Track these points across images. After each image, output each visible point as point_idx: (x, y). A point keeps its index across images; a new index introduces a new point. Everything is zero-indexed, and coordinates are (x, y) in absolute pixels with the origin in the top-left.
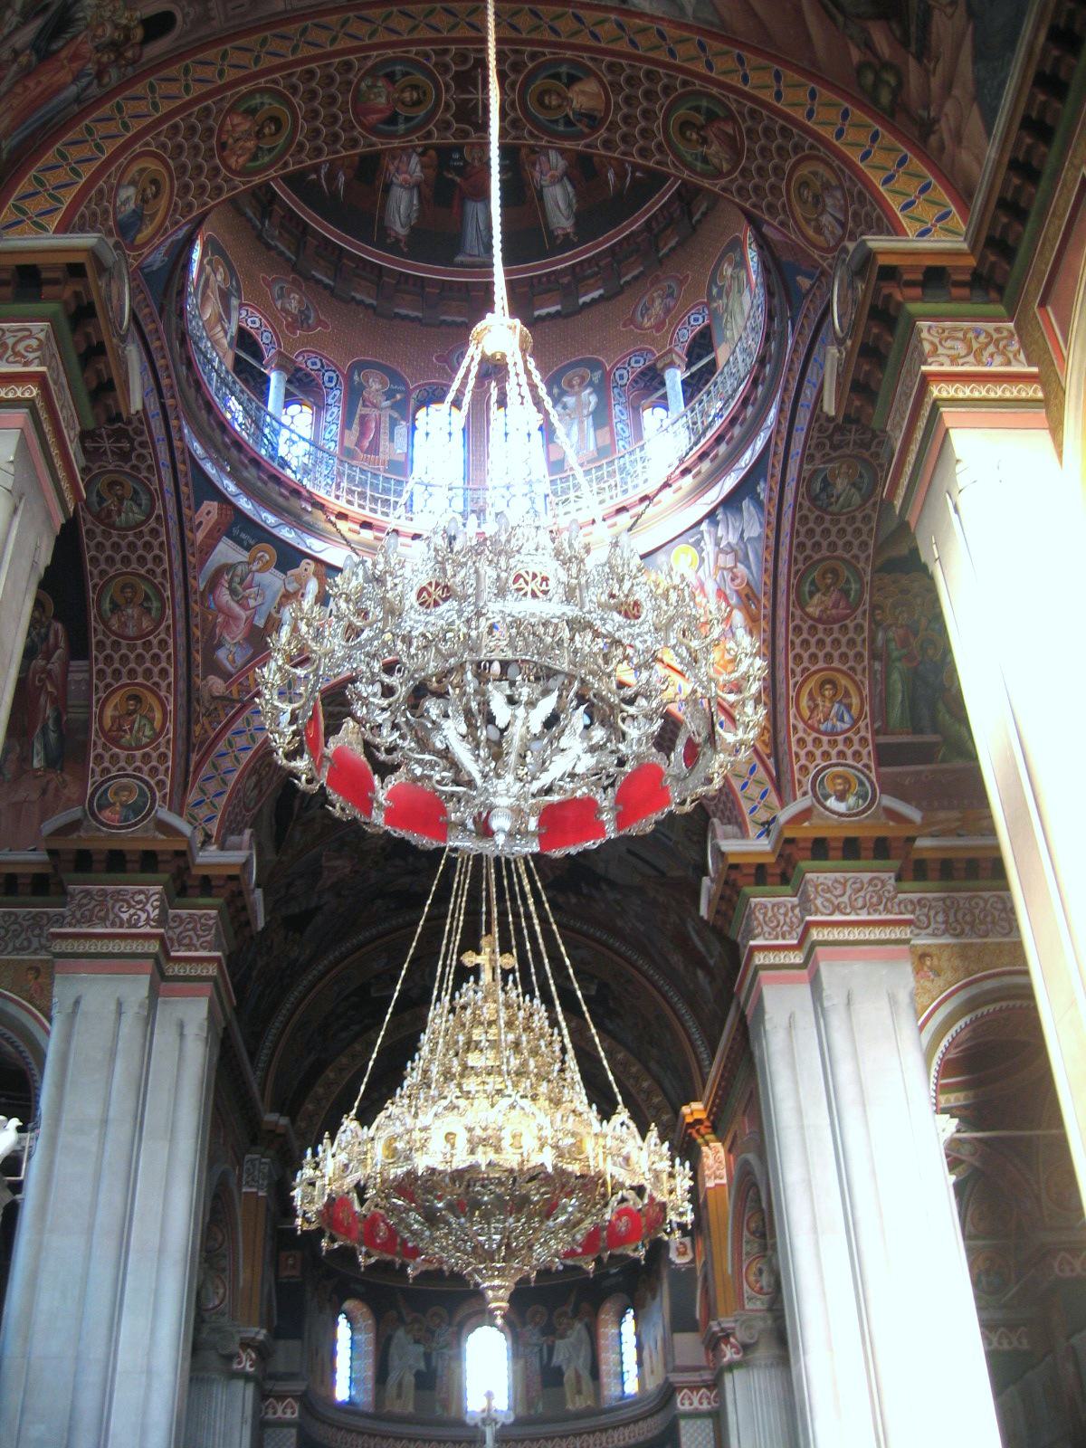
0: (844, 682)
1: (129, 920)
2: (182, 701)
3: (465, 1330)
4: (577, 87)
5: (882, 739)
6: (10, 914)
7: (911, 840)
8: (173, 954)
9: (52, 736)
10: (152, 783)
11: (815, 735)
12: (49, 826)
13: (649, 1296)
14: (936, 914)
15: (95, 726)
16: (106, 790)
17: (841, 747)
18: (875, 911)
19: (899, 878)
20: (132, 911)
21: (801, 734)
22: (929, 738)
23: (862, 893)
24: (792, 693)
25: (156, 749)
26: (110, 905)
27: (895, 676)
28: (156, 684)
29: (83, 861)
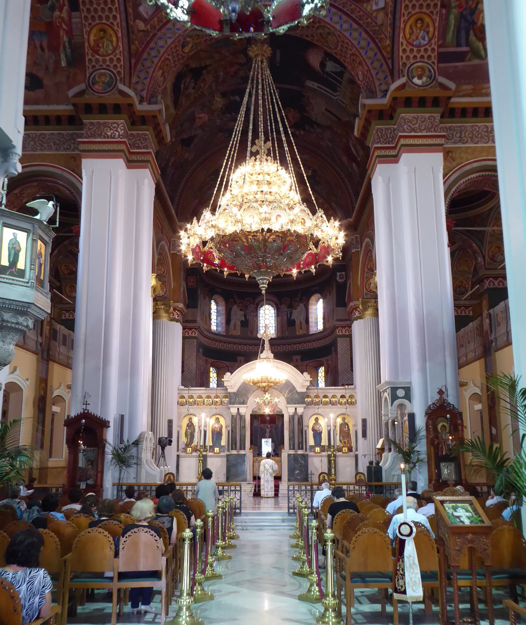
0: (427, 19)
1: (111, 136)
2: (125, 32)
5: (442, 50)
6: (60, 133)
7: (449, 98)
8: (131, 151)
9: (68, 50)
10: (115, 72)
11: (411, 47)
12: (71, 93)
14: (457, 133)
15: (86, 45)
16: (95, 76)
17: (422, 53)
18: (430, 131)
19: (442, 117)
20: (112, 131)
21: (404, 47)
22: (464, 49)
23: (425, 123)
24: (402, 26)
25: (115, 56)
26: (102, 129)
27: (452, 17)
28: (112, 23)
29: (88, 109)
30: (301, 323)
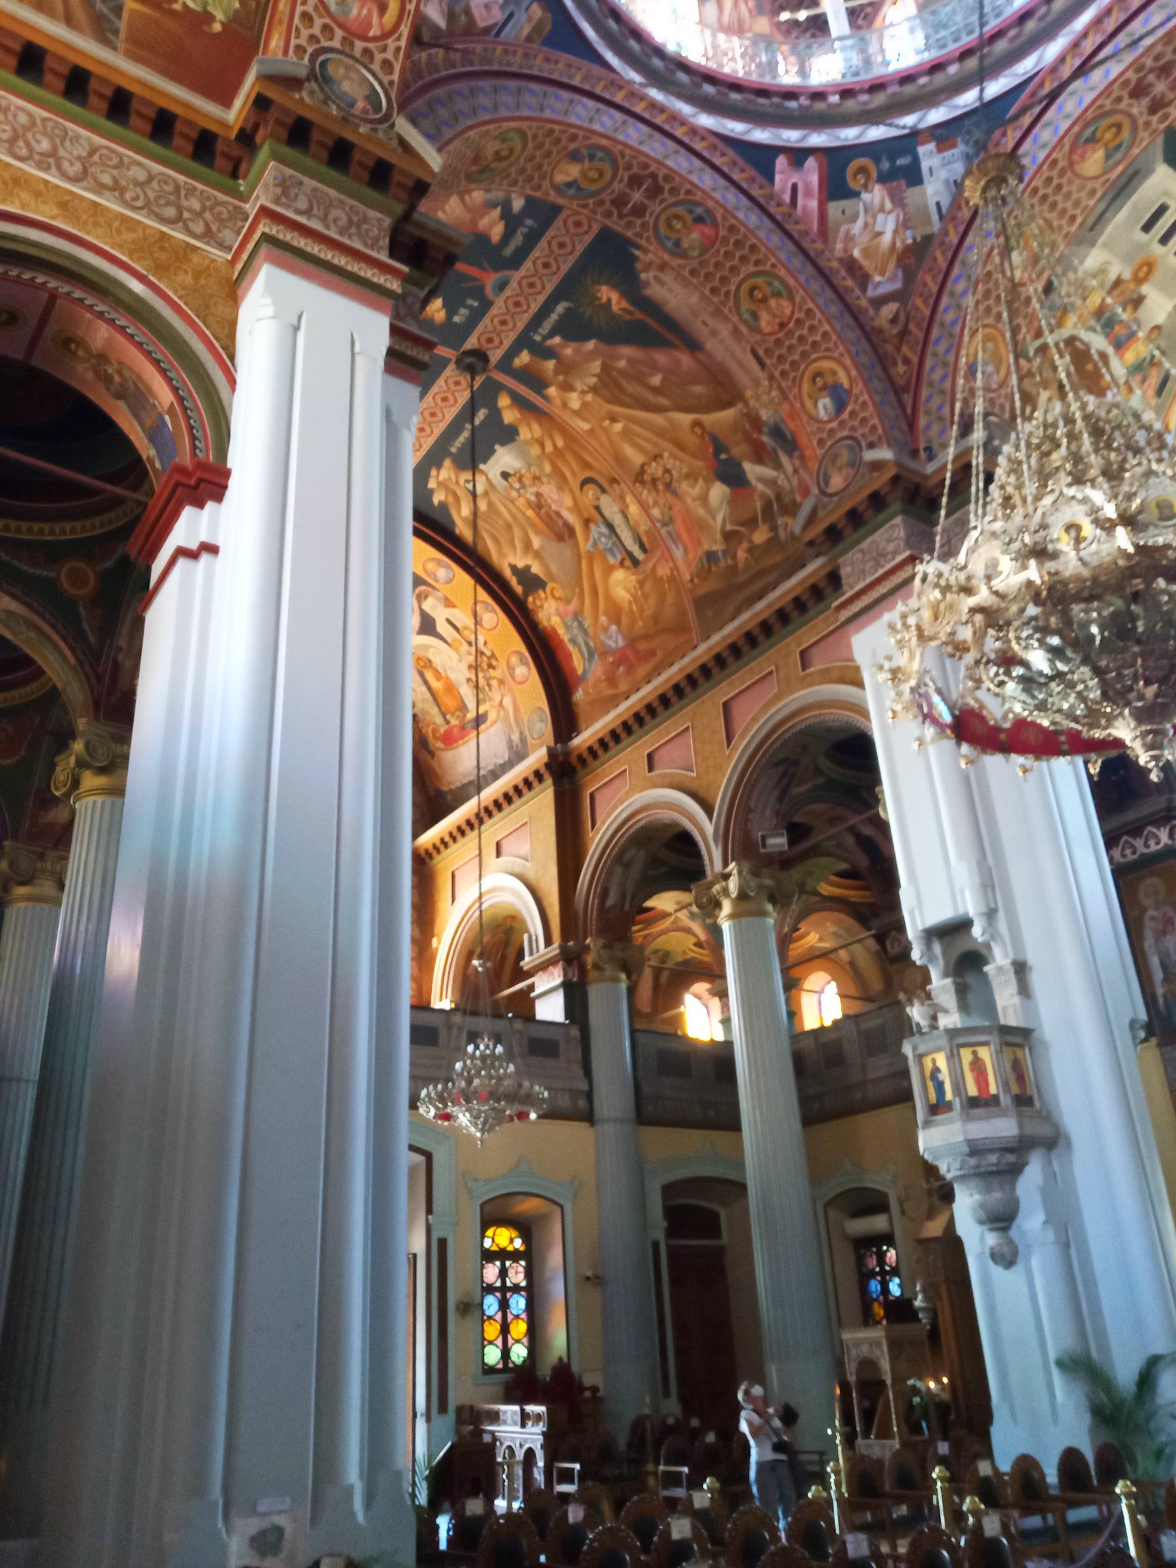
4: (570, 179)
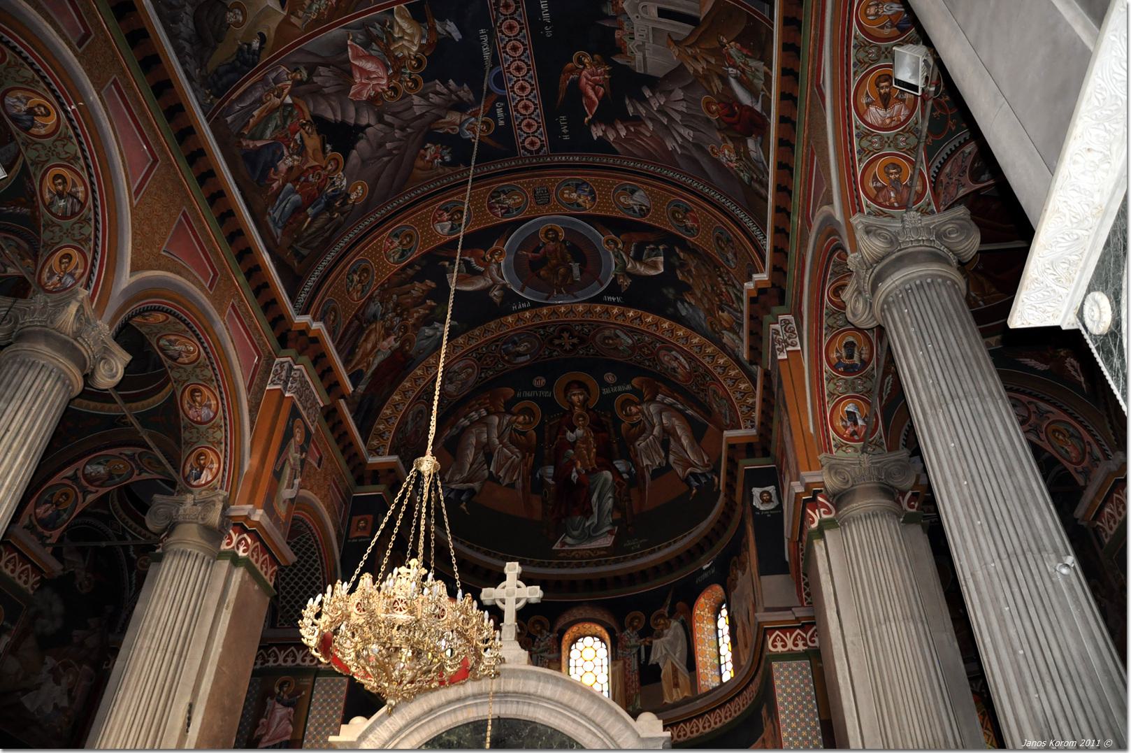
3: (567, 637)
13: (740, 574)
30: (675, 670)
